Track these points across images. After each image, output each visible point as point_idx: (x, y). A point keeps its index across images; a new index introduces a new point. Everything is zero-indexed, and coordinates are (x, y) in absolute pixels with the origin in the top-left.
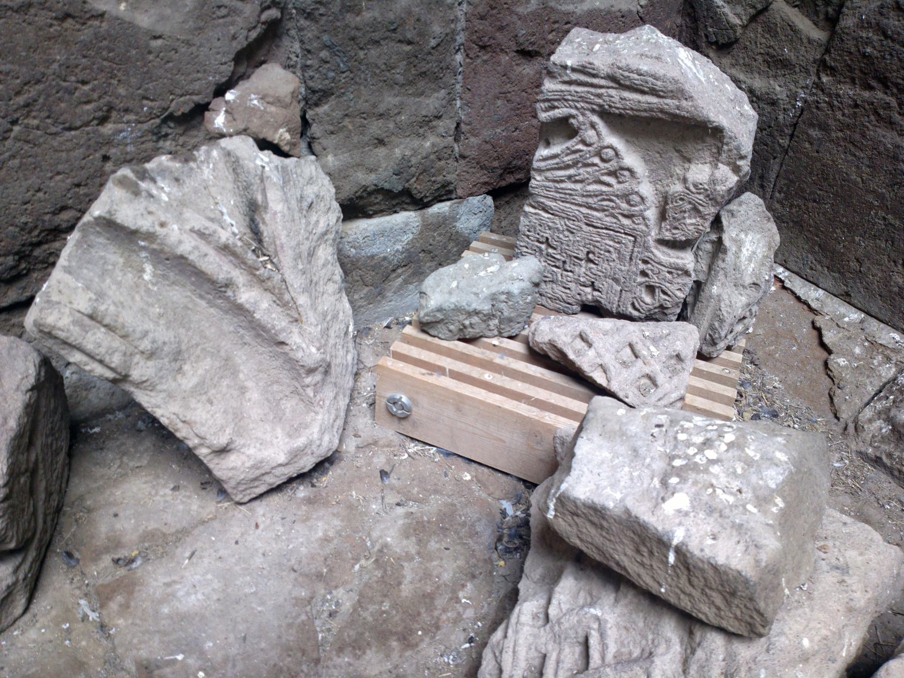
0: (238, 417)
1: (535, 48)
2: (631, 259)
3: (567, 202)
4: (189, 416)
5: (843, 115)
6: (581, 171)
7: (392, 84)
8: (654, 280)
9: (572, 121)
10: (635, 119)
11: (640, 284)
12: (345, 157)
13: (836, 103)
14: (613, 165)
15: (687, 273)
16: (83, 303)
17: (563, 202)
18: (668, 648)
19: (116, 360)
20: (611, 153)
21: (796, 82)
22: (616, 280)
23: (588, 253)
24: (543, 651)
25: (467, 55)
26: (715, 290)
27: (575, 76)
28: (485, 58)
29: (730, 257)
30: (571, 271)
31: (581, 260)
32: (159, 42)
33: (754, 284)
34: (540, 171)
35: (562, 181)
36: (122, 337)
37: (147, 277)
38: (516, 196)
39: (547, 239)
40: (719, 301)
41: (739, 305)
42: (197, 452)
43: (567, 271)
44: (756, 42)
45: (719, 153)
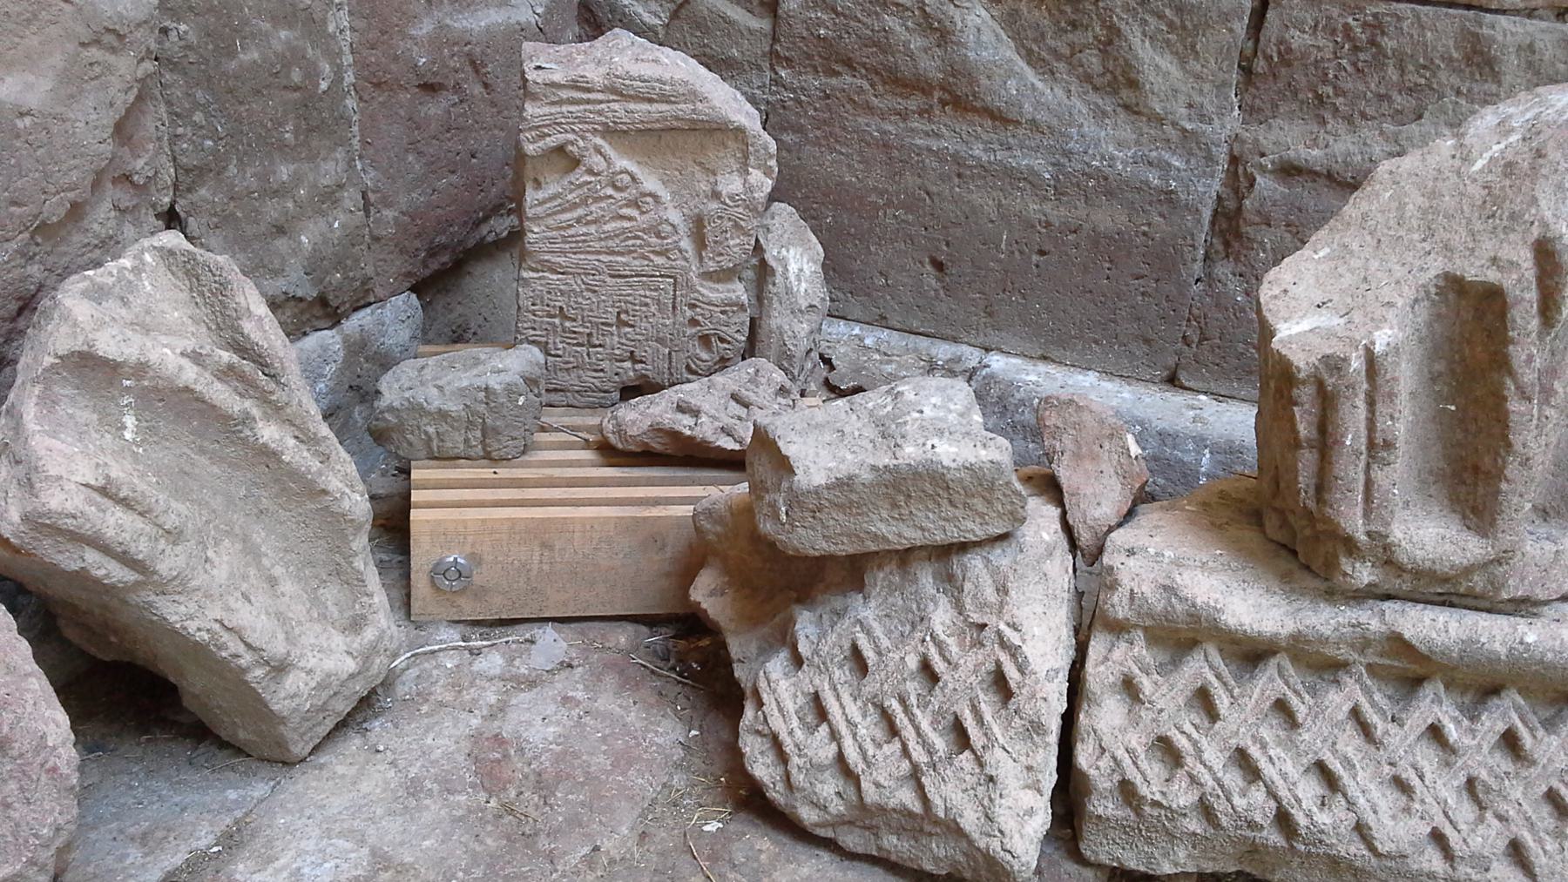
1: (438, 79)
2: (674, 307)
3: (581, 253)
5: (816, 109)
6: (593, 208)
8: (707, 328)
9: (570, 148)
11: (691, 337)
13: (803, 98)
15: (742, 307)
17: (575, 253)
18: (936, 604)
20: (626, 178)
21: (749, 82)
22: (660, 340)
23: (619, 313)
24: (812, 691)
25: (361, 98)
26: (774, 322)
27: (564, 94)
28: (381, 99)
29: (779, 279)
30: (600, 346)
31: (610, 325)
32: (28, 120)
33: (811, 306)
34: (537, 218)
35: (572, 226)
36: (140, 514)
37: (128, 435)
38: (439, 292)
39: (561, 308)
40: (781, 334)
41: (803, 334)
42: (249, 677)
43: (595, 346)
44: (685, 43)
45: (747, 158)
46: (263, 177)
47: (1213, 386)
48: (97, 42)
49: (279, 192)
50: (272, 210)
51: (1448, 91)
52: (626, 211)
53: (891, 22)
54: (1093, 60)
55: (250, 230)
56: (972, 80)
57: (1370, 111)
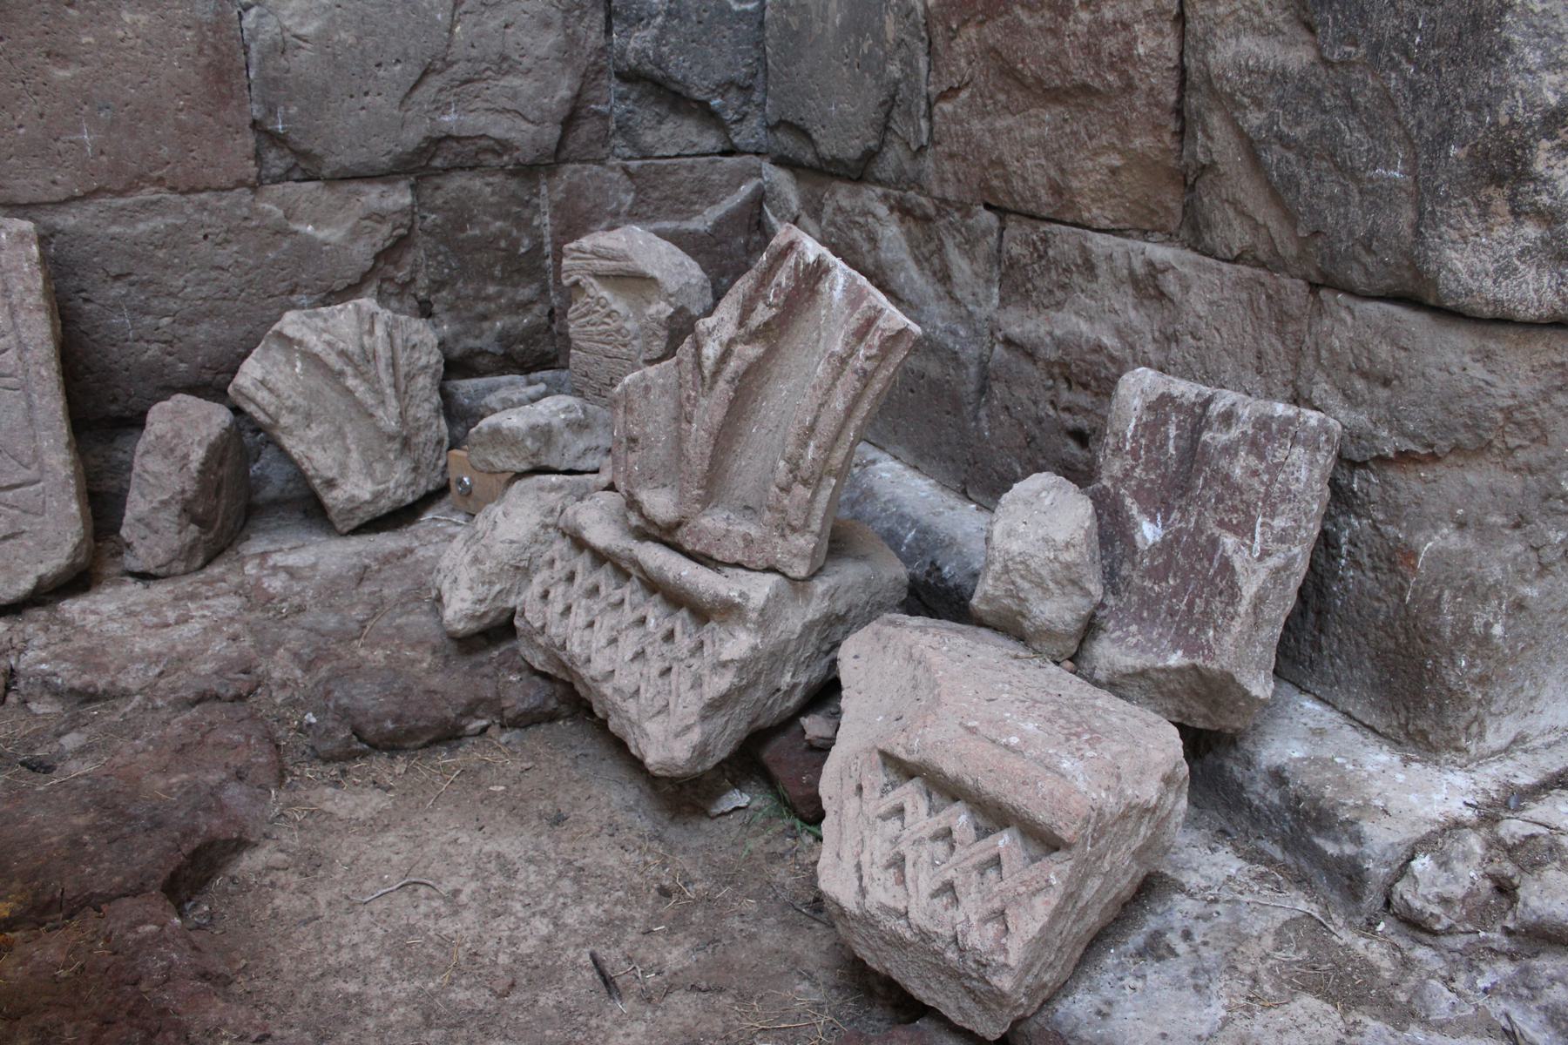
0: (343, 467)
4: (310, 454)
7: (493, 278)
10: (617, 277)
12: (458, 327)
14: (606, 310)
16: (258, 374)
19: (272, 409)
27: (576, 254)
47: (980, 498)
48: (368, 218)
49: (488, 299)
50: (481, 307)
53: (856, 234)
54: (936, 261)
55: (465, 314)
56: (884, 273)
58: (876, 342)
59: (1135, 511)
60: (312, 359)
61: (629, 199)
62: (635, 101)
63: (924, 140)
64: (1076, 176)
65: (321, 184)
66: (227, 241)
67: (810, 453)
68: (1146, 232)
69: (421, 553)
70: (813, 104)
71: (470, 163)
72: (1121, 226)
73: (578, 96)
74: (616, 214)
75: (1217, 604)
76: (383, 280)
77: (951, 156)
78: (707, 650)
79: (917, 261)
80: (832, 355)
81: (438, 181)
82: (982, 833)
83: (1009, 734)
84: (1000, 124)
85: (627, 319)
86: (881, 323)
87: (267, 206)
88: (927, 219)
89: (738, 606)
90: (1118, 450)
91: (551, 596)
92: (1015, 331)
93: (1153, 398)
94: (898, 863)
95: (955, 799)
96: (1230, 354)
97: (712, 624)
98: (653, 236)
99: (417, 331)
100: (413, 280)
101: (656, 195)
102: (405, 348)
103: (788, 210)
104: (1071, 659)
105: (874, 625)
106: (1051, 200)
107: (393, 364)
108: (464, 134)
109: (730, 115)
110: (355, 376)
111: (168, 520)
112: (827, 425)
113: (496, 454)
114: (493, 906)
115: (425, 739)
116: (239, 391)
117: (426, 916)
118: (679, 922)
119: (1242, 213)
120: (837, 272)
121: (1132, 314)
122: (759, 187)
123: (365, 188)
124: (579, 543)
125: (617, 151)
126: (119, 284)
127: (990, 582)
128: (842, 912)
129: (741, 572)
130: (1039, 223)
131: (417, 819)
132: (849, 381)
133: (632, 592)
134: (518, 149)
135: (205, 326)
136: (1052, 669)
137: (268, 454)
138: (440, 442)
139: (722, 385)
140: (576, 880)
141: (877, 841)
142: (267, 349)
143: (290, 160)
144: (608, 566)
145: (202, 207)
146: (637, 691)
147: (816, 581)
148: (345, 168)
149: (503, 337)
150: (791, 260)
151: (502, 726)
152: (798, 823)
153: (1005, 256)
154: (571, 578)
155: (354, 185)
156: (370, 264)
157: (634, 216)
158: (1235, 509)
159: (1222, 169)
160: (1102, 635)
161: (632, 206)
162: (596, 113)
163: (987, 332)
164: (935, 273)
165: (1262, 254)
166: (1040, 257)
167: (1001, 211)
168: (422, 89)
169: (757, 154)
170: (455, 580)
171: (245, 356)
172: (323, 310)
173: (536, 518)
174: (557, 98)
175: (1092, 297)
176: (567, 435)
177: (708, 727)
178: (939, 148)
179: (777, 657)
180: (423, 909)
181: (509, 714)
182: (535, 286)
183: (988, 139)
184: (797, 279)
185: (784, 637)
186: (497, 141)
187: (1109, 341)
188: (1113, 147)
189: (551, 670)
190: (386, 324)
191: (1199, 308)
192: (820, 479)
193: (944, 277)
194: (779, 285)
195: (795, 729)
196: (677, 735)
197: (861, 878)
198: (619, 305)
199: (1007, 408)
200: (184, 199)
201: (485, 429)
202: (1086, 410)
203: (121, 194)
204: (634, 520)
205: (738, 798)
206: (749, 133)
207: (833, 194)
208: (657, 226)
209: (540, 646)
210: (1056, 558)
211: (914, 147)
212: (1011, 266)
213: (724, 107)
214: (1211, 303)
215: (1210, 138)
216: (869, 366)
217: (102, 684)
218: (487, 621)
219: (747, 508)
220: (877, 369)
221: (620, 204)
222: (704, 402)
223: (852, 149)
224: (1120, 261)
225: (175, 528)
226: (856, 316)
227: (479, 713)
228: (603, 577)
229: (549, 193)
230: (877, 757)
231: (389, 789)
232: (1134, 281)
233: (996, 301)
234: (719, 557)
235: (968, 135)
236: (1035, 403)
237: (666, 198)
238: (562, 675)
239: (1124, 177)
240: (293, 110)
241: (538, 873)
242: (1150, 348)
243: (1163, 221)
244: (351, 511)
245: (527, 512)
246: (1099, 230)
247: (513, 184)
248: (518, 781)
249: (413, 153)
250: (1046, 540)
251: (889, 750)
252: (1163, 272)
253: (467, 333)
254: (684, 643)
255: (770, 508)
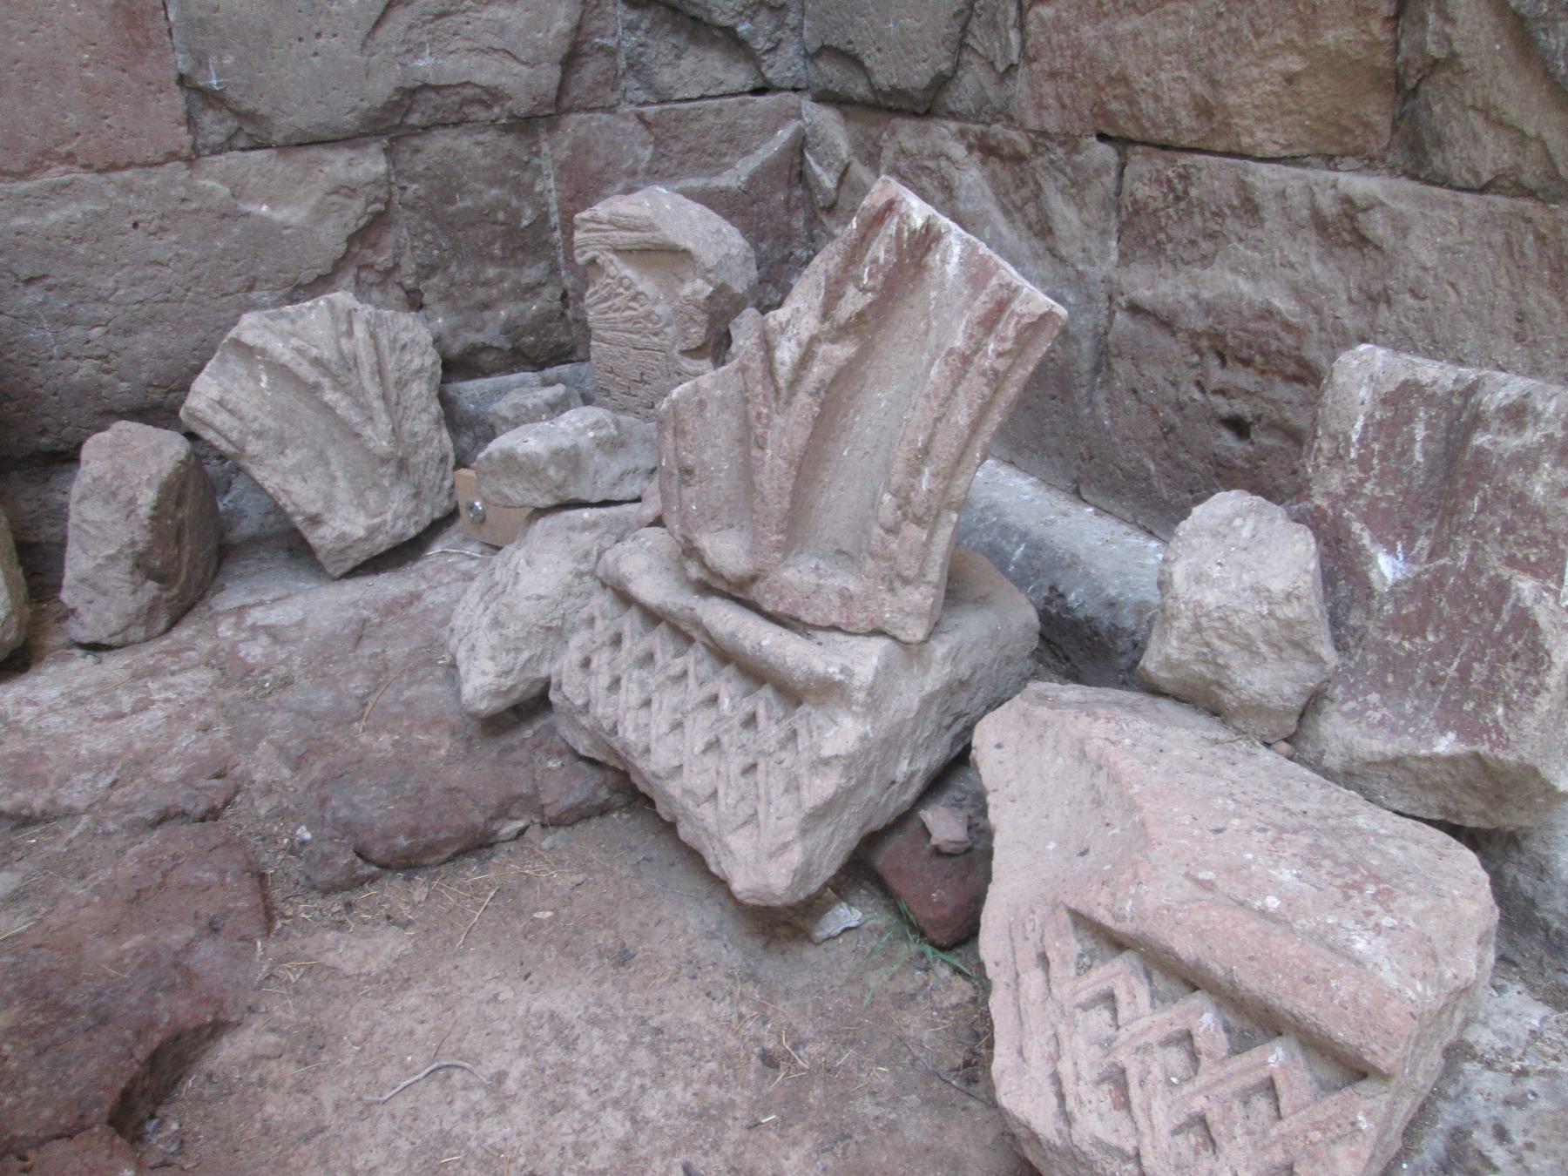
0: (329, 499)
4: (287, 487)
7: (492, 258)
12: (456, 320)
16: (214, 393)
19: (235, 435)
34: (590, 306)
46: (476, 275)
47: (1100, 500)
48: (335, 192)
50: (480, 294)
51: (1233, 238)
52: (632, 304)
54: (1031, 210)
55: (462, 304)
57: (1186, 256)
58: (1011, 332)
59: (1366, 540)
60: (280, 371)
61: (647, 153)
62: (647, 32)
63: (1014, 58)
64: (1234, 89)
65: (273, 152)
66: (163, 229)
67: (925, 483)
68: (1331, 158)
69: (431, 598)
70: (864, 22)
71: (454, 118)
72: (1296, 151)
73: (578, 28)
74: (633, 173)
75: (1509, 672)
76: (361, 268)
77: (1053, 75)
78: (803, 741)
79: (1006, 212)
80: (951, 352)
81: (416, 142)
82: (1240, 1043)
83: (1263, 893)
84: (1123, 27)
85: (656, 302)
86: (1017, 306)
87: (209, 183)
88: (1019, 158)
89: (839, 684)
90: (1338, 458)
91: (594, 665)
92: (1144, 295)
93: (1391, 387)
94: (1117, 1079)
95: (1195, 988)
96: (1470, 316)
97: (805, 708)
98: (680, 198)
99: (406, 328)
100: (397, 266)
101: (678, 147)
102: (393, 350)
103: (836, 156)
104: (1286, 740)
105: (1017, 703)
106: (1195, 124)
107: (380, 371)
108: (443, 82)
109: (761, 44)
110: (335, 389)
111: (118, 577)
112: (946, 446)
113: (512, 486)
114: (549, 1095)
115: (449, 852)
116: (192, 415)
117: (465, 1116)
118: (793, 1107)
119: (1501, 125)
120: (952, 238)
121: (1317, 268)
122: (799, 131)
123: (327, 154)
124: (625, 599)
125: (630, 95)
126: (32, 289)
127: (1175, 643)
128: (1034, 1137)
129: (839, 637)
130: (1176, 155)
131: (445, 967)
132: (975, 385)
133: (698, 662)
134: (510, 98)
135: (147, 335)
136: (1266, 756)
137: (239, 485)
138: (443, 460)
139: (802, 398)
140: (654, 1049)
141: (1080, 1042)
142: (223, 361)
143: (232, 124)
144: (662, 627)
145: (127, 188)
146: (714, 794)
147: (933, 643)
148: (302, 132)
149: (509, 329)
150: (891, 227)
151: (543, 826)
152: (929, 950)
153: (1127, 200)
154: (617, 641)
155: (314, 152)
156: (342, 248)
157: (655, 174)
158: (1533, 542)
159: (1466, 63)
160: (1328, 707)
161: (651, 161)
162: (601, 48)
163: (1103, 297)
164: (1030, 226)
165: (1529, 179)
166: (1178, 199)
167: (1122, 143)
168: (387, 26)
169: (795, 90)
170: (473, 648)
171: (197, 370)
172: (289, 309)
173: (568, 566)
174: (553, 32)
175: (1255, 248)
176: (598, 458)
177: (809, 842)
178: (1035, 66)
179: (890, 744)
180: (459, 1105)
181: (551, 812)
182: (543, 265)
183: (1105, 49)
184: (900, 253)
185: (898, 718)
186: (486, 89)
187: (1283, 304)
188: (1290, 45)
189: (600, 757)
190: (368, 322)
191: (1424, 256)
192: (938, 515)
193: (1043, 230)
194: (875, 261)
195: (912, 826)
196: (771, 856)
197: (1061, 1097)
198: (646, 286)
199: (1135, 391)
200: (102, 179)
201: (497, 455)
202: (1247, 392)
203: (23, 176)
204: (694, 571)
205: (845, 915)
206: (784, 65)
207: (894, 133)
208: (681, 184)
209: (583, 728)
210: (1271, 613)
211: (1001, 68)
212: (1136, 213)
213: (754, 34)
214: (1443, 249)
215: (1449, 19)
216: (1001, 365)
217: (39, 803)
218: (515, 696)
219: (840, 552)
220: (1011, 368)
221: (637, 161)
222: (779, 420)
223: (918, 76)
224: (1297, 199)
225: (127, 588)
226: (983, 298)
227: (514, 813)
228: (657, 640)
229: (553, 150)
230: (1065, 917)
231: (407, 924)
232: (1320, 223)
233: (1114, 257)
234: (808, 619)
235: (1078, 48)
236: (1175, 384)
237: (690, 150)
238: (613, 762)
239: (1305, 86)
240: (229, 60)
241: (607, 1040)
242: (1344, 311)
243: (1360, 141)
244: (342, 551)
245: (555, 558)
246: (1264, 160)
247: (508, 142)
248: (568, 901)
249: (384, 109)
250: (1256, 590)
251: (1084, 909)
252: (1365, 210)
253: (467, 325)
254: (770, 732)
255: (873, 555)
